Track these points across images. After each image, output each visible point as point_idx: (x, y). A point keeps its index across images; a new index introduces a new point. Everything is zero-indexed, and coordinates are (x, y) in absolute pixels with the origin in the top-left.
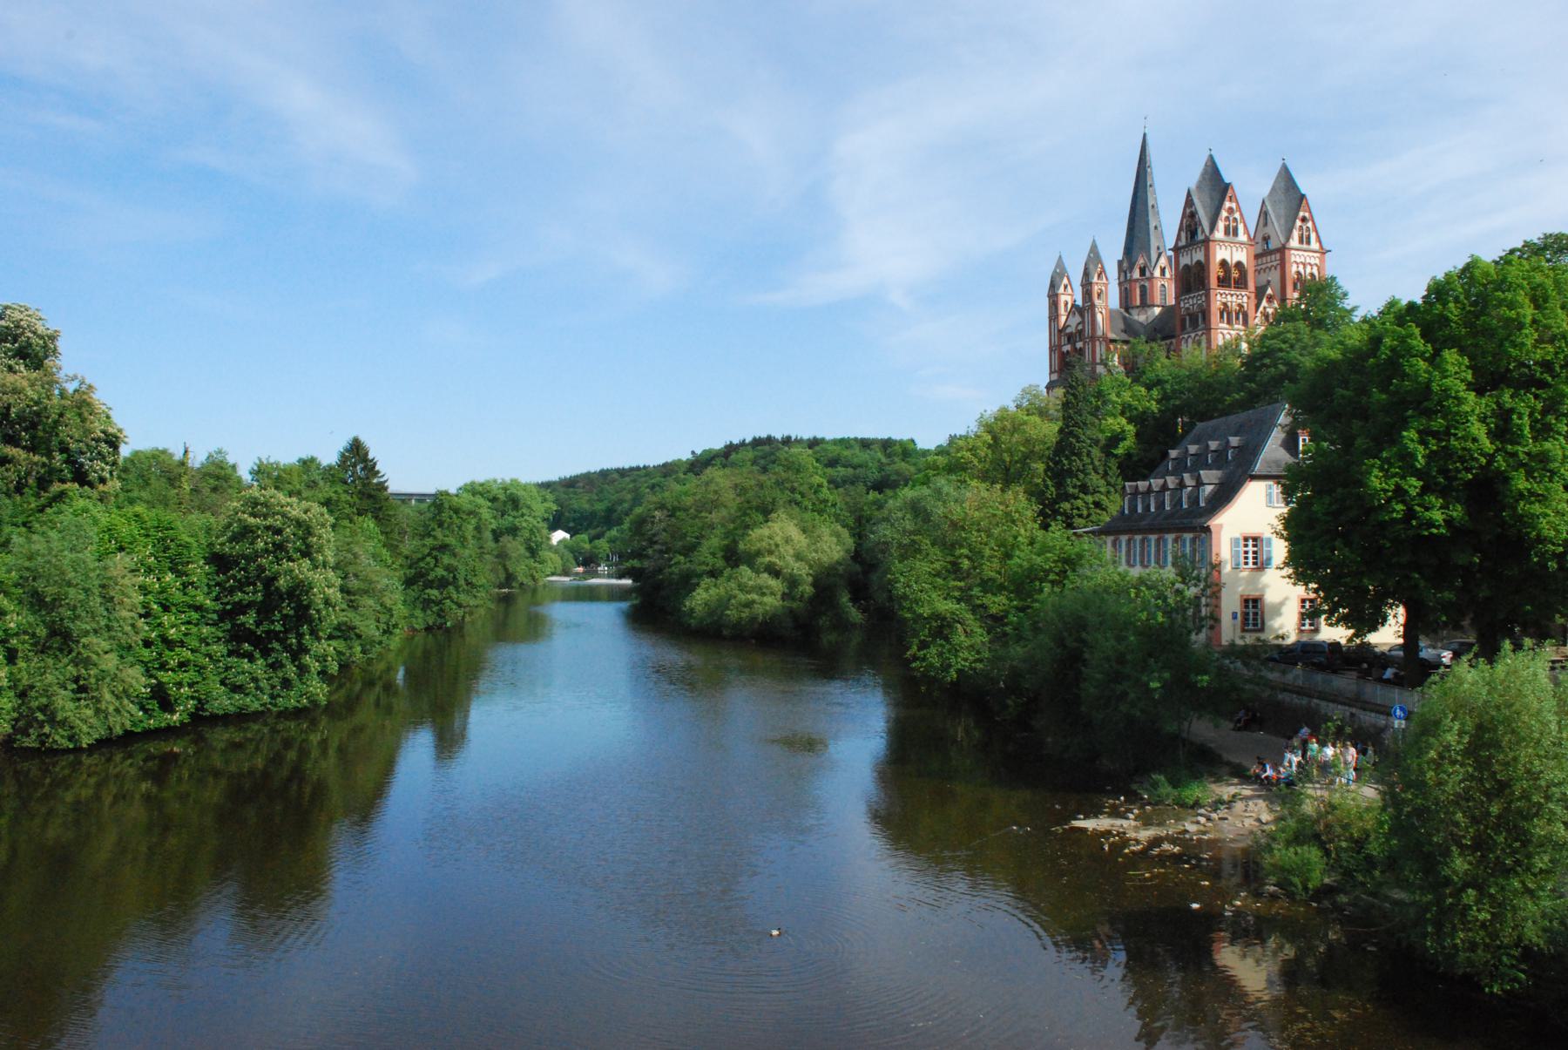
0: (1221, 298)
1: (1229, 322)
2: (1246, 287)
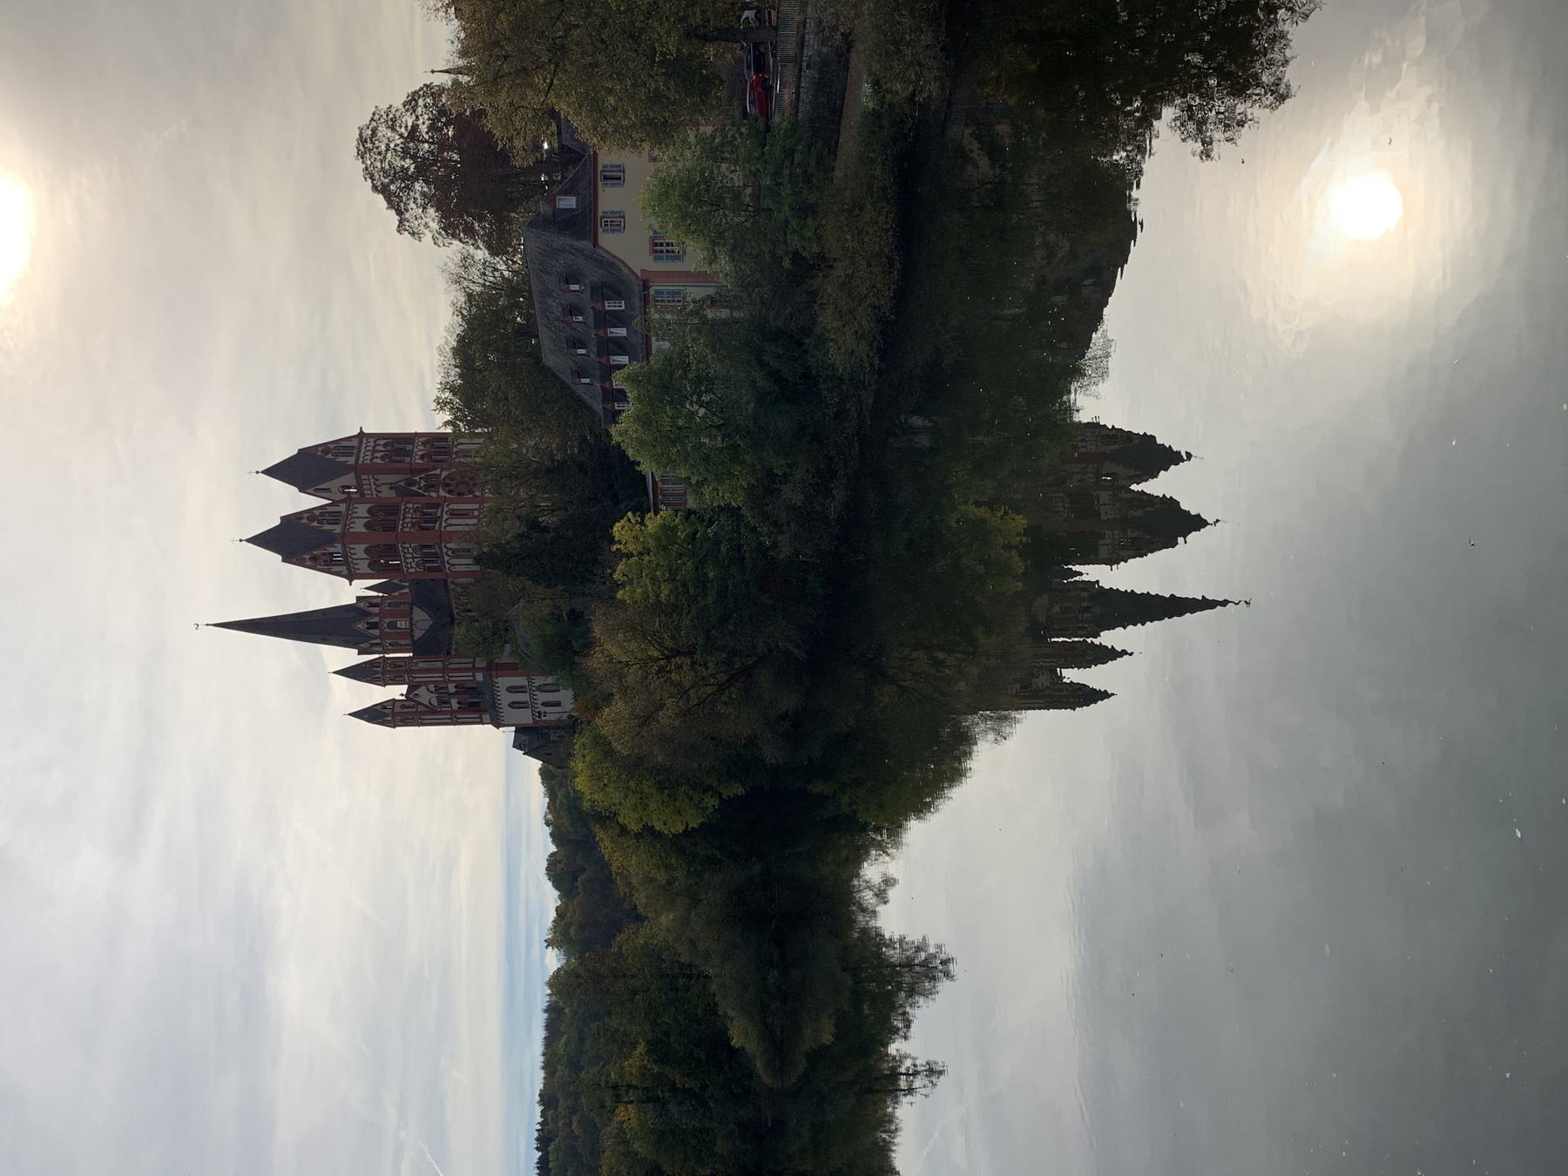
2: (398, 506)
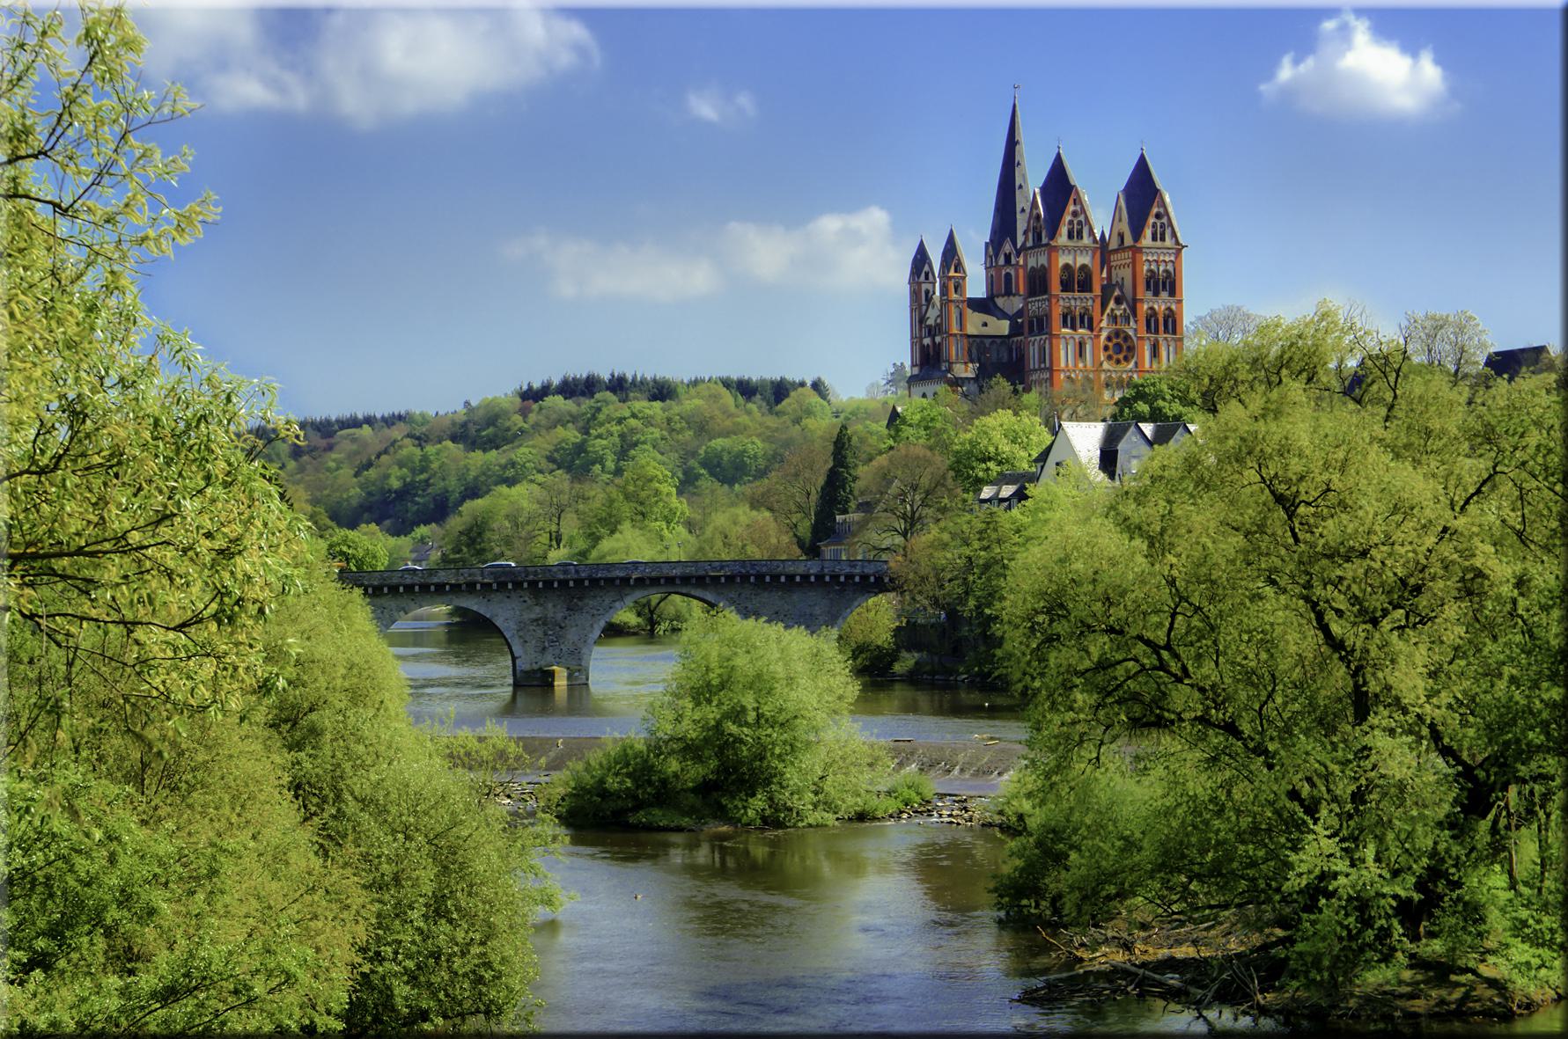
0: (1062, 300)
1: (1073, 328)
2: (1090, 291)
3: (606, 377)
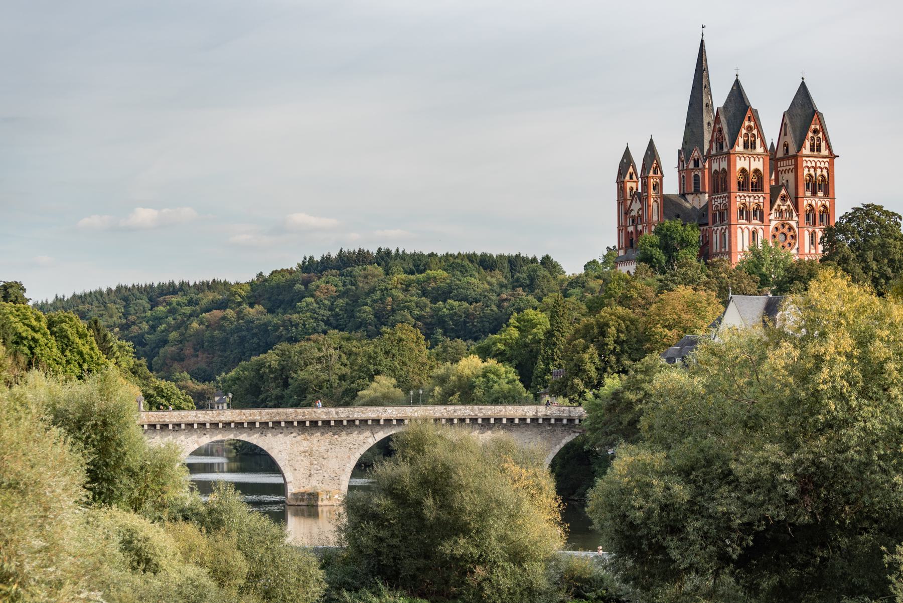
0: (739, 199)
1: (747, 219)
2: (762, 190)
3: (374, 251)
